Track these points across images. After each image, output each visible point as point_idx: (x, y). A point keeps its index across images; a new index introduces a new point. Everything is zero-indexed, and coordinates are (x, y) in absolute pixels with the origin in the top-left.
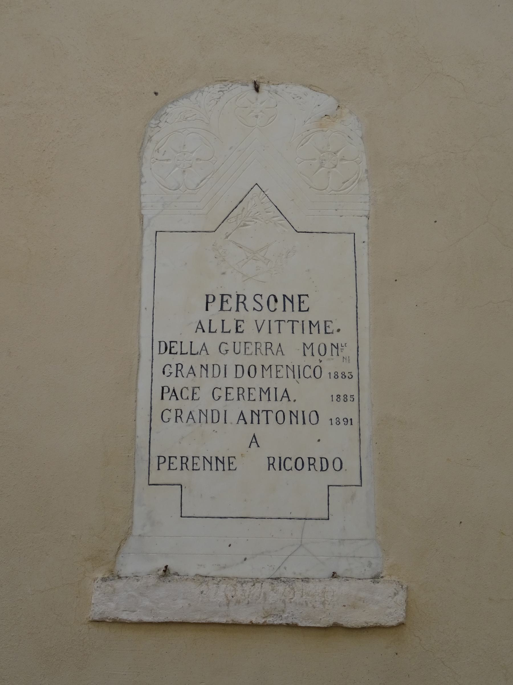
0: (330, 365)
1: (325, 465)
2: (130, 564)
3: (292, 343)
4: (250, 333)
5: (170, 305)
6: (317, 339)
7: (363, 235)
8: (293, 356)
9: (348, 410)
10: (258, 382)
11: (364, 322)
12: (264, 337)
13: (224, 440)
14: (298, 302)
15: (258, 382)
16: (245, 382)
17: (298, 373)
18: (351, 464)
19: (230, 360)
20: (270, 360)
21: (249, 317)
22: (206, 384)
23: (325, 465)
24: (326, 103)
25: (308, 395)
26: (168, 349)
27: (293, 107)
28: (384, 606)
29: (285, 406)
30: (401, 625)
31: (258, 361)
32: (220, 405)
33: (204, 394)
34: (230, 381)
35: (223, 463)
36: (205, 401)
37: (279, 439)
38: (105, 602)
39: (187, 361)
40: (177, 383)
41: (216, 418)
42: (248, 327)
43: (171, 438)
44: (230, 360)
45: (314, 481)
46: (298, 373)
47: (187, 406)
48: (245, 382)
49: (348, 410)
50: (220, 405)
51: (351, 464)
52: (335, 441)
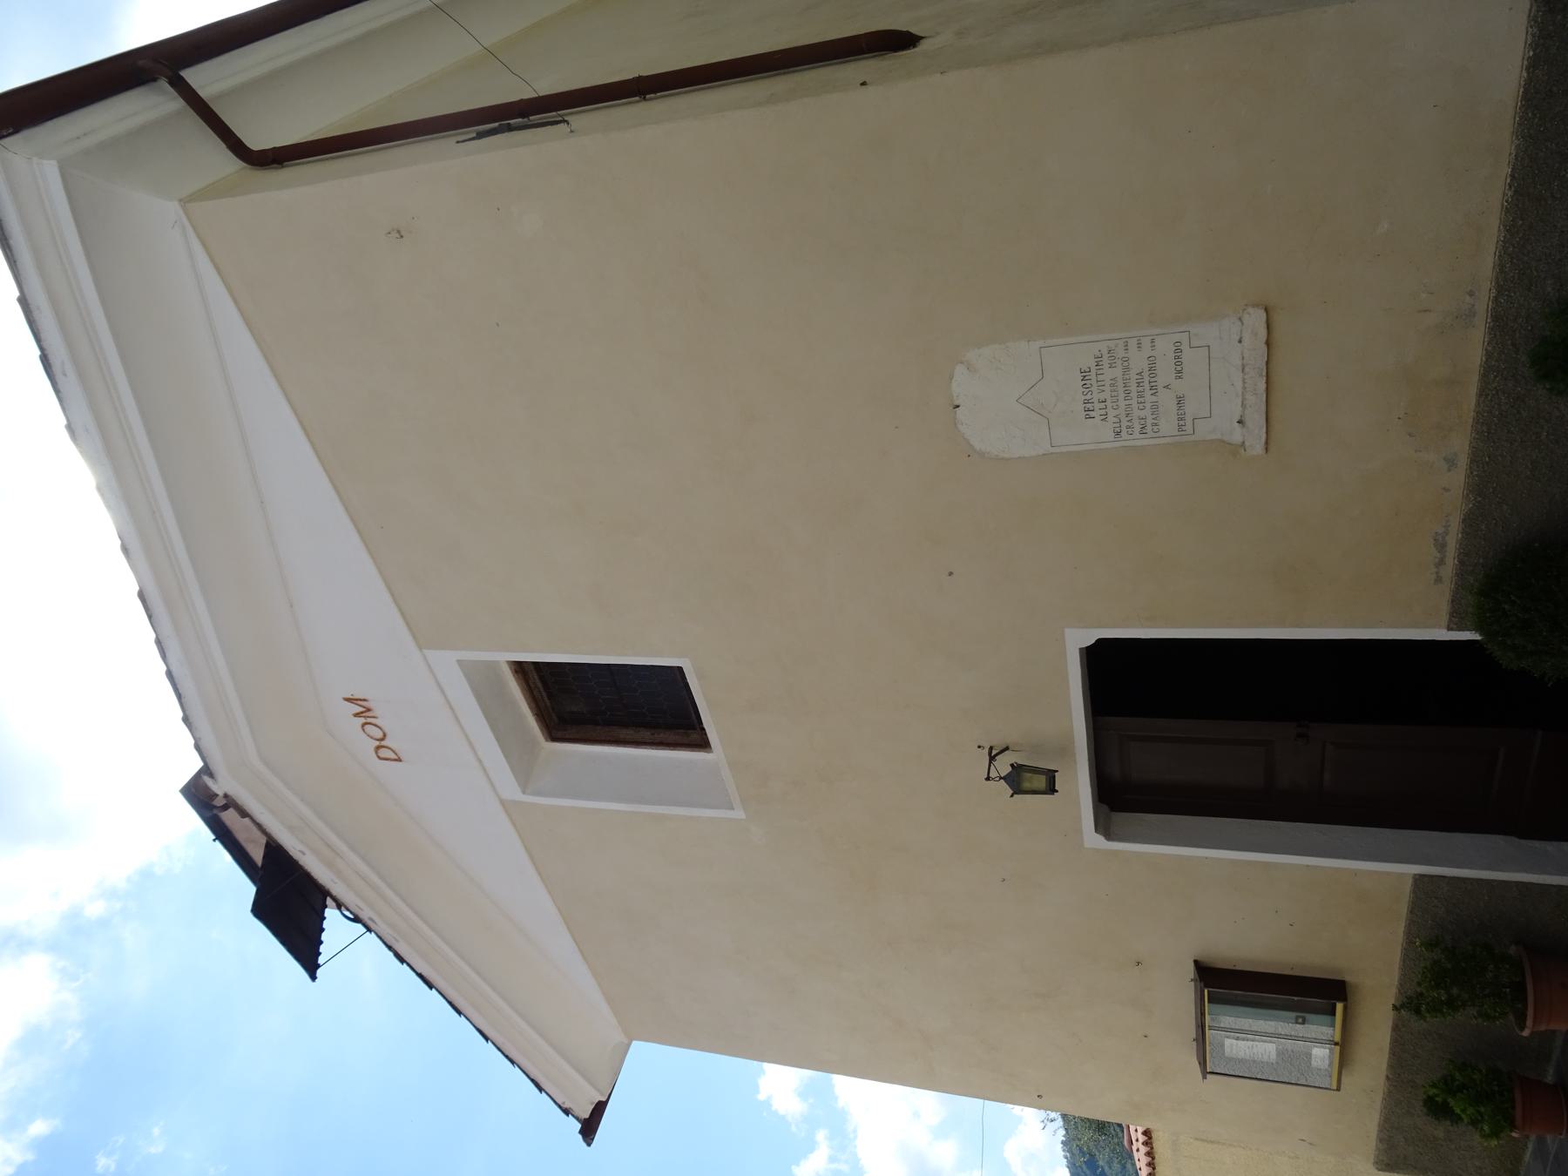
0: (1121, 353)
1: (1178, 350)
2: (1237, 435)
3: (1109, 374)
4: (1106, 395)
5: (1096, 435)
6: (1105, 361)
7: (1040, 343)
8: (1118, 372)
9: (1146, 342)
10: (1133, 387)
11: (1094, 338)
12: (1107, 388)
13: (1167, 400)
15: (1133, 387)
16: (1134, 394)
17: (1127, 369)
18: (1177, 337)
19: (1122, 403)
20: (1120, 383)
21: (1096, 397)
22: (1136, 413)
23: (1178, 350)
24: (960, 370)
25: (1139, 362)
26: (1118, 433)
27: (962, 385)
28: (1256, 318)
29: (1146, 374)
30: (1266, 310)
31: (1121, 389)
32: (1148, 405)
33: (1142, 414)
34: (1134, 402)
35: (1180, 401)
36: (1147, 413)
37: (1165, 374)
38: (1258, 448)
39: (1125, 423)
40: (1137, 428)
41: (1155, 407)
42: (1102, 397)
43: (1168, 426)
44: (1122, 403)
45: (1187, 354)
46: (1127, 369)
47: (1150, 421)
48: (1134, 394)
49: (1146, 342)
50: (1148, 405)
51: (1177, 337)
52: (1165, 346)
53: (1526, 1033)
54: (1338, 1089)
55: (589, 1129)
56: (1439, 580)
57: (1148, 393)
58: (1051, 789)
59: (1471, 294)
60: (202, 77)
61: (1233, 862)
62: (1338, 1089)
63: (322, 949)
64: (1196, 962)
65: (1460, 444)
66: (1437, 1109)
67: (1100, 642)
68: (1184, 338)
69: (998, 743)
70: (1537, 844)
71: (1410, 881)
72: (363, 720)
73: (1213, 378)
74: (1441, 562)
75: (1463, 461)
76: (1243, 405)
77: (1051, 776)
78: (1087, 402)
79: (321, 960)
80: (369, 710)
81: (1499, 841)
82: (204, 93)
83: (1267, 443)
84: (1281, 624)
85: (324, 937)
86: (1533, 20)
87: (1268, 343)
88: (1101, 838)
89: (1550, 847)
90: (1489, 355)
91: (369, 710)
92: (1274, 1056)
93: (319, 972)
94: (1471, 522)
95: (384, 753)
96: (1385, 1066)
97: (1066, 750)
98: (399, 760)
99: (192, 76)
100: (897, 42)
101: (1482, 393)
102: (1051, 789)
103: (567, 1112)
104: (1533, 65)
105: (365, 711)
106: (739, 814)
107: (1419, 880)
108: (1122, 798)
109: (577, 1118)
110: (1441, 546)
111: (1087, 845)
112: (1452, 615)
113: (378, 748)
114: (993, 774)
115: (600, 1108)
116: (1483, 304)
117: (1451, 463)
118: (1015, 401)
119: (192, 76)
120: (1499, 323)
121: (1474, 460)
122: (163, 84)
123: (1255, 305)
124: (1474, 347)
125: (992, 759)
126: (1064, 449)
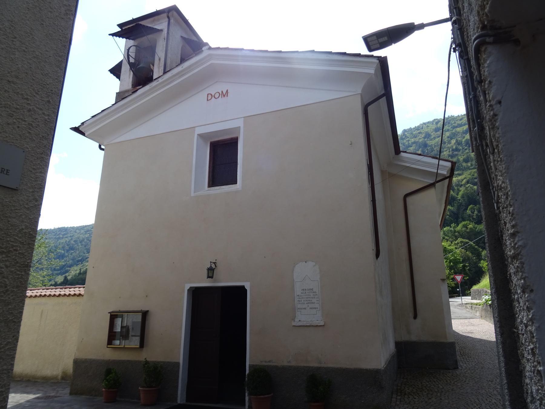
0: (316, 297)
1: (316, 308)
2: (296, 320)
3: (312, 294)
5: (298, 291)
8: (312, 296)
14: (312, 289)
23: (316, 308)
24: (314, 263)
25: (314, 300)
27: (311, 264)
35: (305, 309)
37: (311, 306)
38: (294, 324)
41: (304, 303)
43: (299, 306)
45: (315, 310)
52: (317, 306)
53: (140, 388)
55: (76, 129)
56: (261, 362)
58: (209, 277)
60: (383, 100)
61: (182, 320)
63: (118, 38)
64: (148, 311)
65: (293, 364)
66: (109, 372)
71: (177, 361)
72: (221, 93)
73: (309, 315)
74: (266, 362)
77: (212, 277)
79: (114, 37)
80: (224, 96)
81: (186, 382)
85: (121, 38)
87: (317, 326)
88: (188, 288)
89: (185, 393)
91: (224, 96)
92: (117, 331)
93: (111, 36)
95: (210, 97)
97: (215, 281)
98: (208, 100)
99: (385, 98)
100: (377, 255)
102: (209, 277)
103: (83, 123)
104: (366, 370)
105: (225, 94)
106: (193, 194)
107: (178, 364)
108: (196, 294)
110: (269, 362)
115: (83, 134)
116: (323, 365)
117: (289, 362)
118: (306, 275)
119: (385, 98)
120: (319, 368)
121: (290, 366)
122: (383, 92)
125: (214, 263)
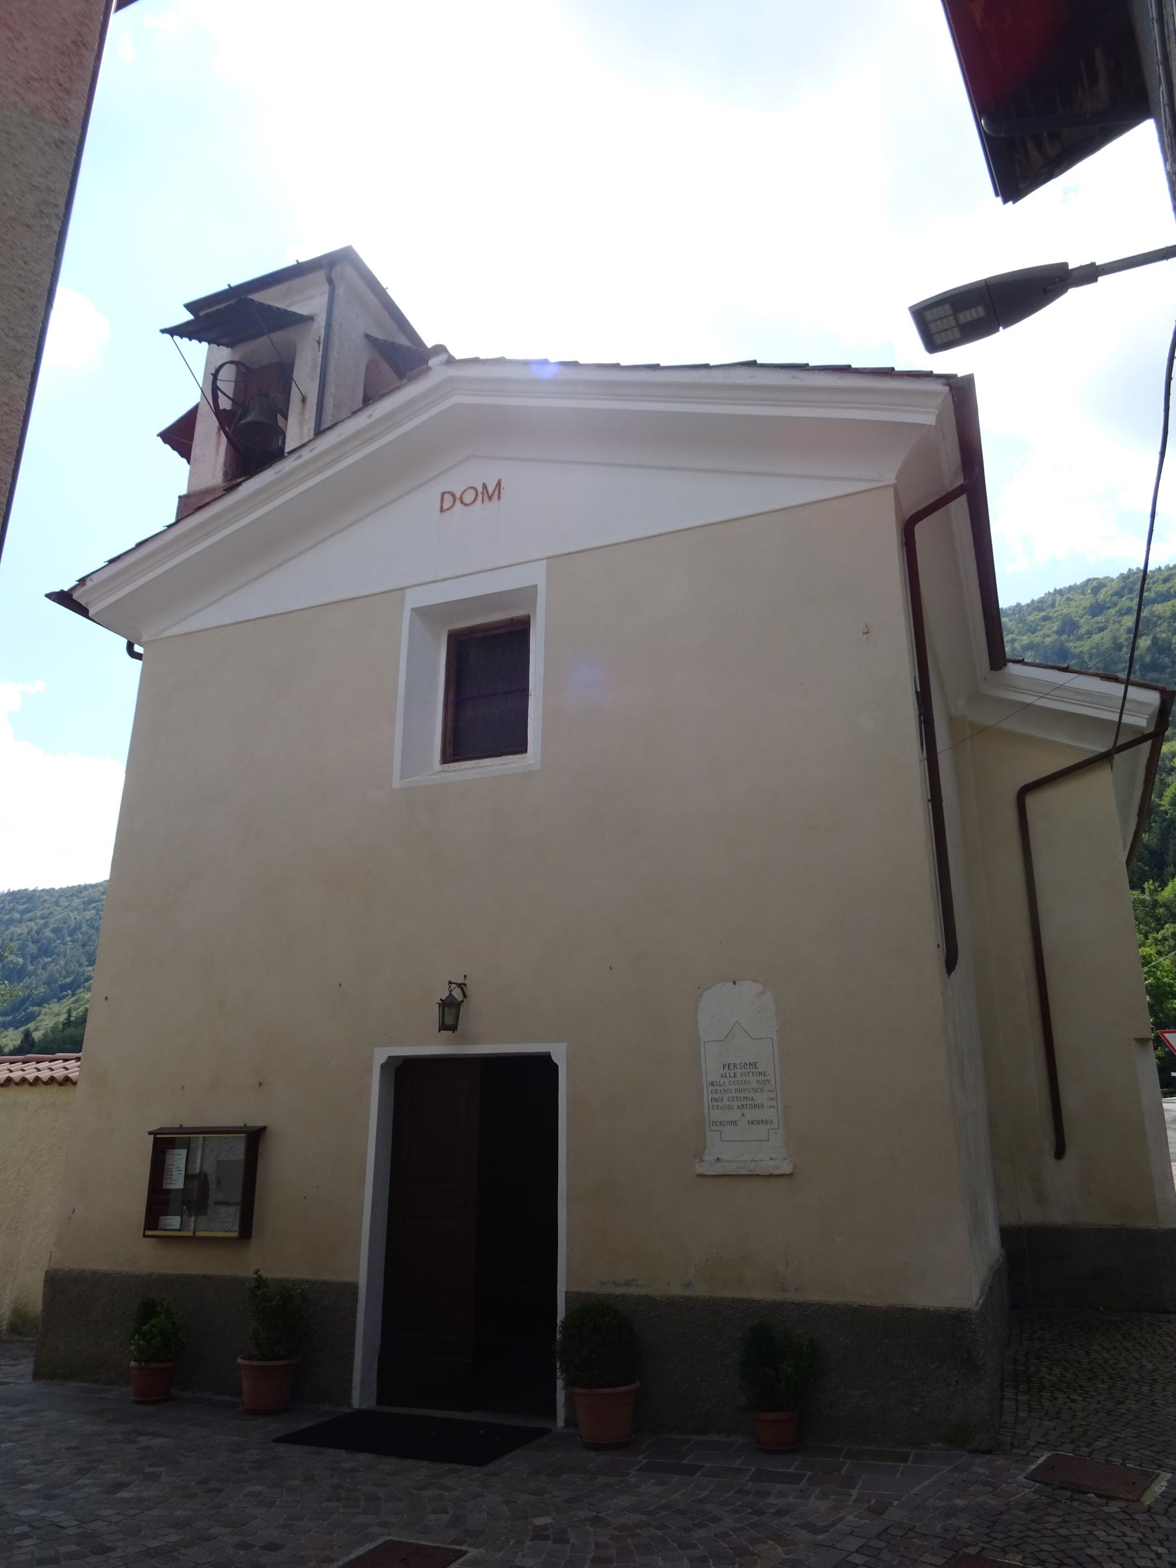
0: (767, 1087)
1: (766, 1122)
2: (707, 1157)
3: (753, 1080)
4: (739, 1077)
5: (712, 1070)
6: (762, 1078)
7: (775, 1038)
8: (754, 1085)
9: (773, 1103)
10: (743, 1095)
11: (777, 1070)
12: (744, 1078)
13: (734, 1115)
14: (753, 1065)
15: (743, 1095)
16: (739, 1095)
17: (756, 1091)
18: (775, 1121)
19: (733, 1087)
20: (746, 1086)
21: (738, 1071)
22: (726, 1096)
23: (766, 1122)
24: (760, 987)
25: (760, 1098)
26: (712, 1084)
28: (786, 1168)
29: (752, 1102)
30: (791, 1174)
31: (742, 1087)
32: (731, 1103)
33: (725, 1099)
34: (734, 1095)
35: (733, 1123)
36: (726, 1102)
37: (751, 1114)
38: (700, 1169)
39: (719, 1088)
40: (716, 1096)
41: (730, 1108)
42: (738, 1075)
43: (716, 1115)
44: (733, 1087)
46: (756, 1091)
47: (720, 1104)
48: (739, 1095)
49: (773, 1103)
50: (731, 1103)
51: (775, 1121)
53: (240, 1361)
54: (145, 1236)
55: (64, 598)
56: (603, 1283)
57: (739, 1103)
58: (443, 1027)
59: (796, 1289)
60: (962, 502)
61: (364, 1157)
62: (145, 1236)
63: (186, 340)
64: (265, 1128)
65: (700, 1290)
66: (148, 1310)
67: (556, 1067)
68: (775, 1126)
69: (468, 991)
70: (376, 1367)
71: (351, 1280)
72: (480, 490)
73: (746, 1143)
74: (616, 1284)
75: (688, 1293)
76: (730, 1161)
77: (453, 1028)
78: (735, 1066)
79: (177, 338)
80: (490, 498)
81: (378, 1341)
82: (953, 505)
83: (704, 1176)
84: (570, 1188)
85: (195, 342)
86: (949, 1309)
87: (770, 1176)
88: (384, 1060)
89: (374, 1376)
90: (759, 1301)
91: (490, 498)
92: (173, 1187)
93: (167, 336)
94: (649, 1301)
95: (448, 501)
96: (163, 1271)
97: (464, 1040)
98: (442, 510)
99: (963, 499)
100: (951, 962)
101: (734, 1300)
102: (443, 1027)
103: (82, 581)
104: (926, 1311)
105: (491, 493)
106: (396, 783)
107: (353, 1288)
108: (408, 1077)
109: (74, 589)
110: (628, 1284)
111: (376, 1049)
112: (579, 1294)
113: (453, 495)
114: (453, 986)
115: (82, 611)
116: (790, 1296)
117: (688, 1285)
118: (735, 1021)
119: (963, 499)
120: (778, 1307)
121: (689, 1299)
122: (960, 481)
123: (794, 1167)
124: (760, 1294)
125: (460, 986)
126: (702, 1049)
